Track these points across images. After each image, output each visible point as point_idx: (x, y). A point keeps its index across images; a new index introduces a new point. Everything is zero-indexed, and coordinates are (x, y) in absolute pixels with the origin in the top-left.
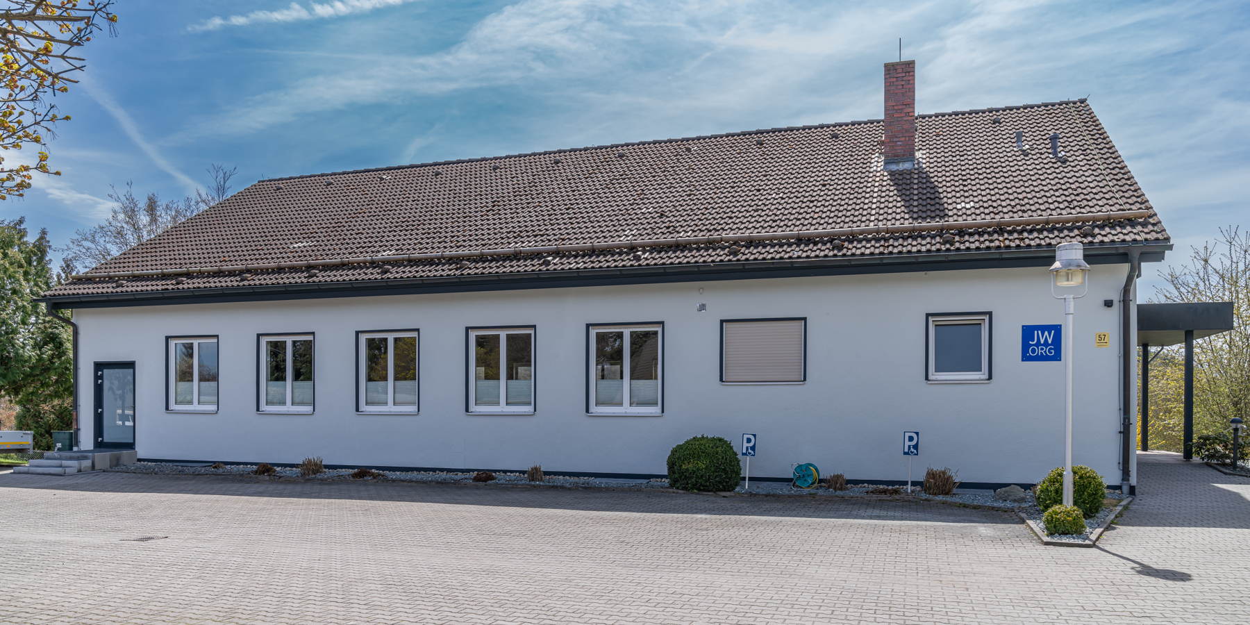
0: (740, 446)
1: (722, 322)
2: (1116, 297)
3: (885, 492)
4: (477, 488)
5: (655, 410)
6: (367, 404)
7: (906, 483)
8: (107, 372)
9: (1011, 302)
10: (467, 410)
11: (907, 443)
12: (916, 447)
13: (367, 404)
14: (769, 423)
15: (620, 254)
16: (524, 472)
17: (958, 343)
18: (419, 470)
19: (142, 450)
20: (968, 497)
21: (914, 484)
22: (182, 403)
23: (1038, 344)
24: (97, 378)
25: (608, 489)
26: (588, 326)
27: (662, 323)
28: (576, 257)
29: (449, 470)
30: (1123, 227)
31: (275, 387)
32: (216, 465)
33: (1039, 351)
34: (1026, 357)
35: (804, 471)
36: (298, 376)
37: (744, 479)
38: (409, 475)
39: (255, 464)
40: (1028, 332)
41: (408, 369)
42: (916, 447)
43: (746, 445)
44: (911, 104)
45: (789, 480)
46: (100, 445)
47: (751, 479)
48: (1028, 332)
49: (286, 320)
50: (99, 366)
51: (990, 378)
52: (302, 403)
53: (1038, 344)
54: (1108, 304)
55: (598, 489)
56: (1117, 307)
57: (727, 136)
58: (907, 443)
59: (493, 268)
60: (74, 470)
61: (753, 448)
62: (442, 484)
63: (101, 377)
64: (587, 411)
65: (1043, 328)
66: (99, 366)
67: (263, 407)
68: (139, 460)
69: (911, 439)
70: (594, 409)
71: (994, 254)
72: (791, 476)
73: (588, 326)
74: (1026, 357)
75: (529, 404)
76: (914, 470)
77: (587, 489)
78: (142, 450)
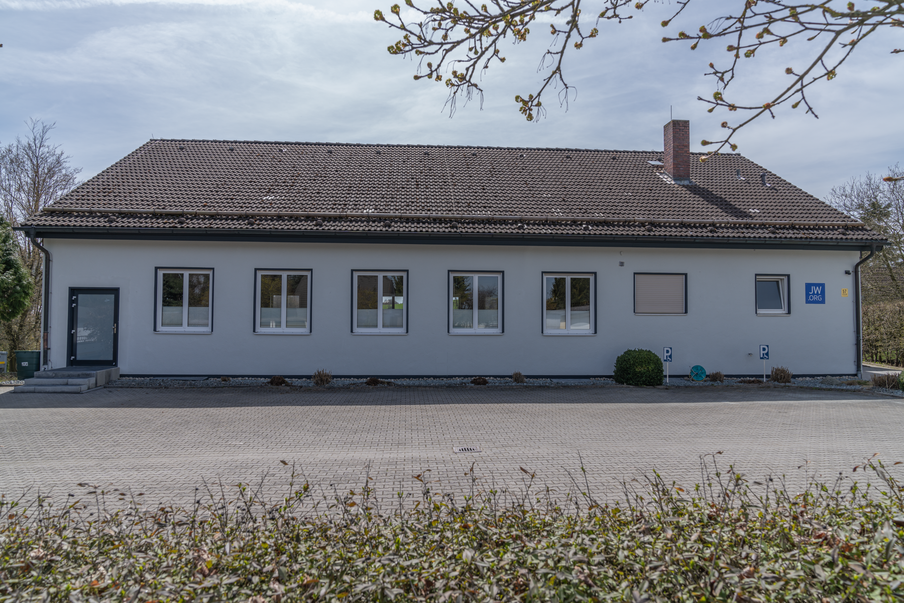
0: (662, 356)
1: (686, 275)
2: (851, 269)
3: (750, 382)
4: (318, 391)
5: (402, 331)
6: (358, 326)
7: (762, 376)
8: (81, 297)
9: (801, 268)
10: (155, 330)
11: (762, 352)
12: (767, 354)
13: (358, 326)
14: (682, 343)
15: (566, 225)
16: (309, 377)
17: (770, 292)
18: (409, 377)
19: (125, 365)
20: (726, 381)
21: (768, 376)
22: (459, 326)
23: (814, 294)
24: (71, 302)
25: (575, 387)
26: (256, 270)
27: (311, 270)
28: (146, 218)
29: (435, 377)
30: (501, 225)
31: (172, 311)
32: (225, 378)
33: (814, 298)
34: (808, 302)
35: (698, 370)
36: (196, 301)
37: (666, 376)
38: (422, 382)
39: (366, 377)
40: (808, 287)
41: (200, 298)
42: (767, 354)
43: (666, 354)
44: (688, 146)
45: (688, 376)
46: (73, 362)
47: (670, 376)
48: (808, 287)
49: (473, 261)
50: (74, 292)
51: (789, 312)
52: (493, 327)
53: (814, 294)
54: (847, 273)
55: (566, 387)
56: (852, 274)
57: (244, 142)
58: (762, 352)
59: (413, 228)
60: (84, 388)
61: (670, 356)
62: (450, 387)
63: (76, 301)
64: (254, 331)
65: (816, 285)
66: (74, 292)
67: (160, 328)
68: (122, 376)
69: (668, 352)
70: (357, 330)
71: (798, 242)
72: (689, 373)
73: (352, 271)
74: (808, 302)
75: (207, 325)
76: (765, 368)
77: (558, 388)
78: (125, 365)
